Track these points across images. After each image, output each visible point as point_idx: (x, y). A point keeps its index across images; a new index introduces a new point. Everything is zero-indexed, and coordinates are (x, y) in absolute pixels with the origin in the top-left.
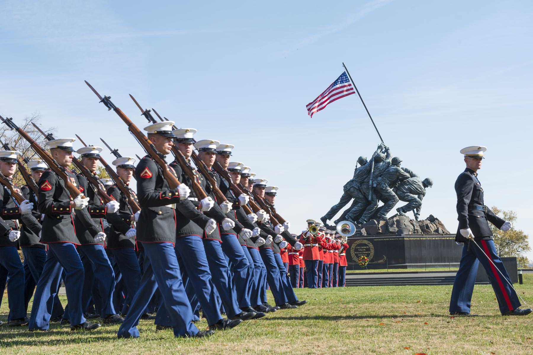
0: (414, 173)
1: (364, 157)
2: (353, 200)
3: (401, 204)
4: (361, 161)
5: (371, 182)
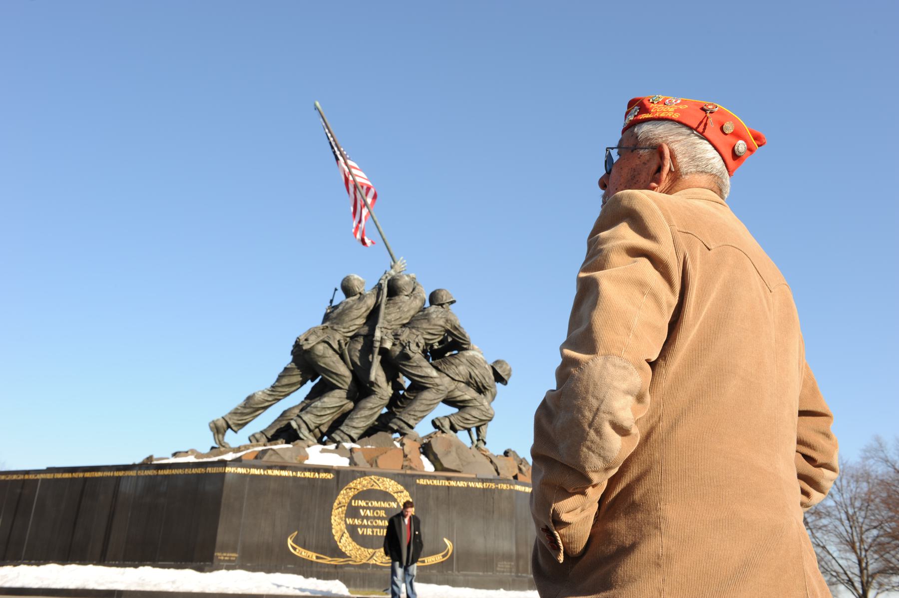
2: (310, 385)
3: (443, 410)
5: (378, 334)
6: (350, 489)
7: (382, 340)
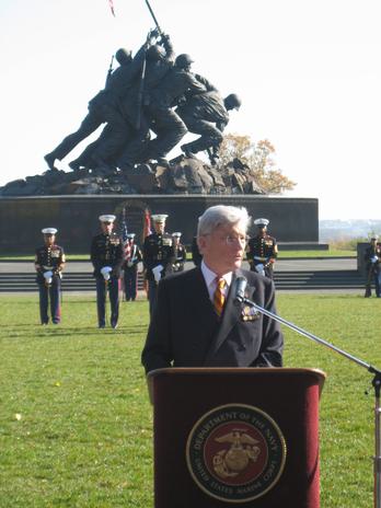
0: (211, 83)
1: (127, 49)
2: (102, 126)
3: (190, 137)
4: (121, 55)
5: (140, 96)
7: (143, 101)
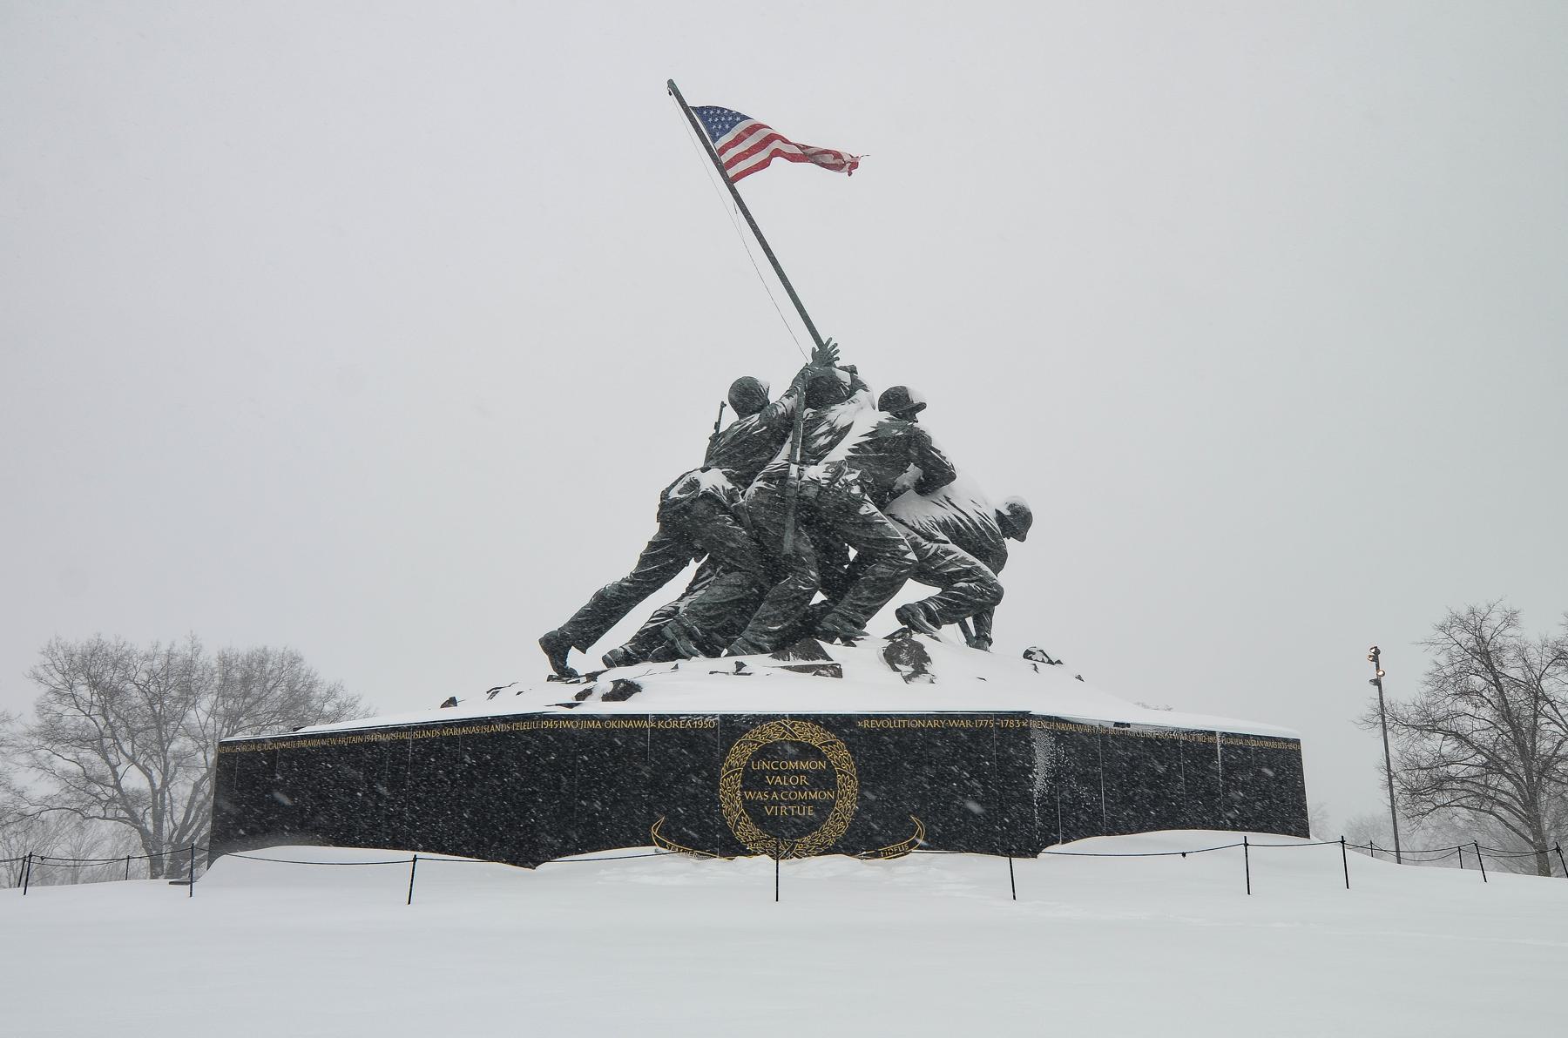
1: (762, 378)
3: (913, 592)
4: (747, 396)
6: (746, 743)
